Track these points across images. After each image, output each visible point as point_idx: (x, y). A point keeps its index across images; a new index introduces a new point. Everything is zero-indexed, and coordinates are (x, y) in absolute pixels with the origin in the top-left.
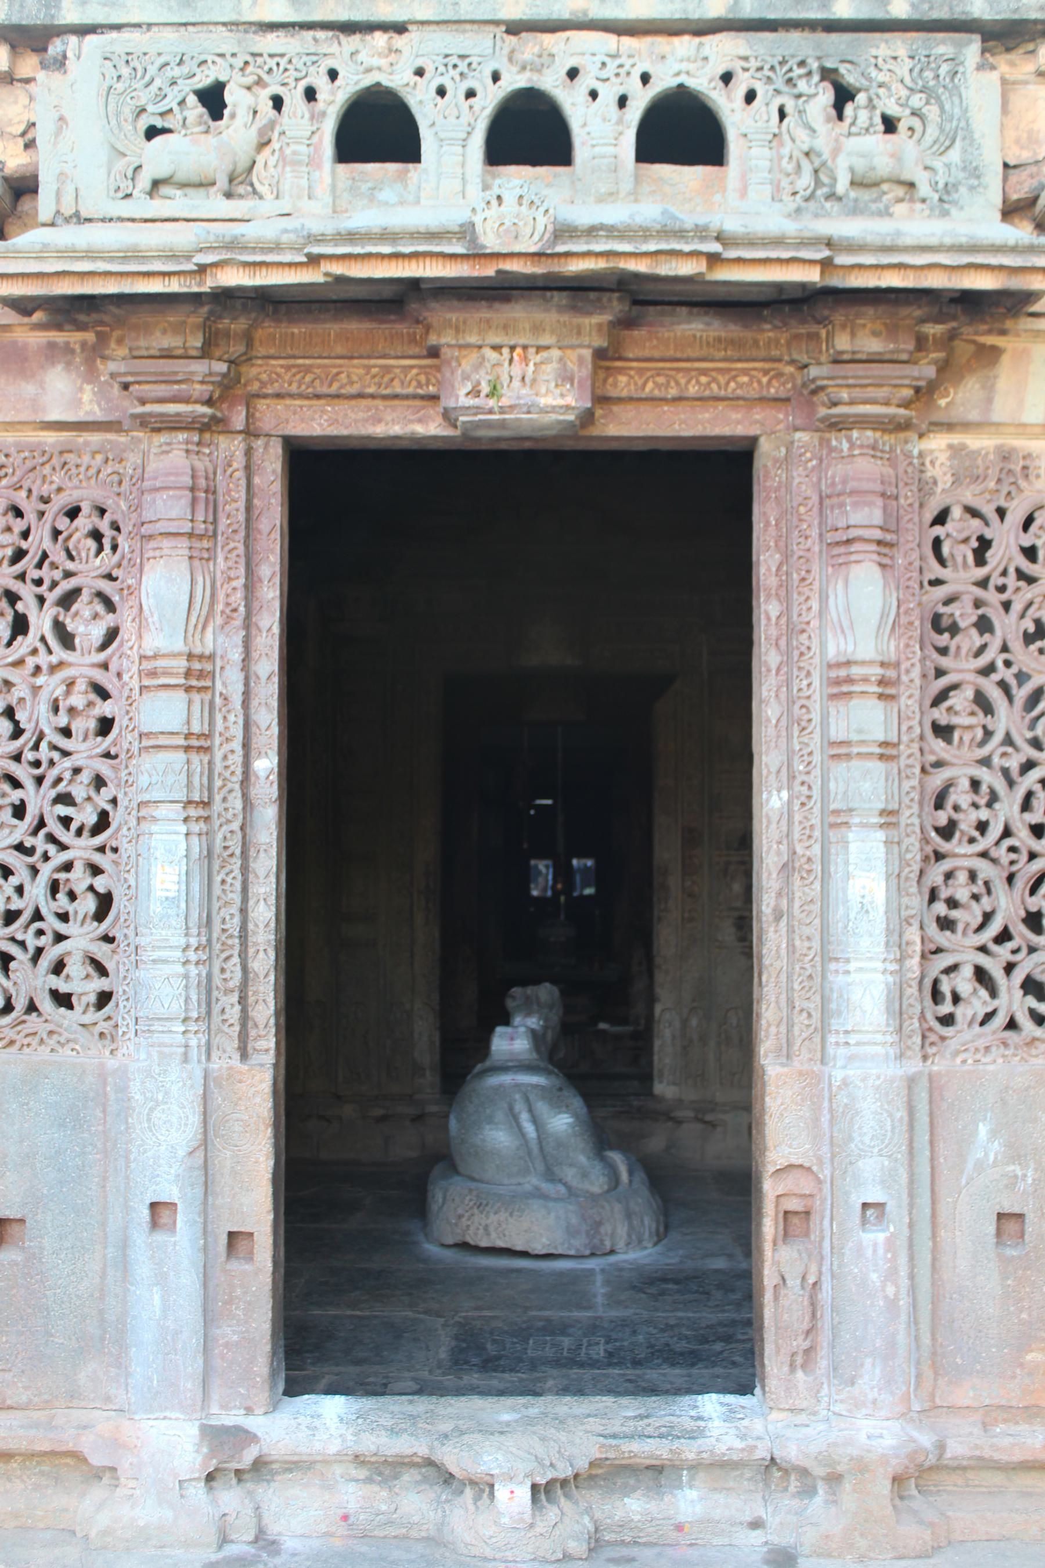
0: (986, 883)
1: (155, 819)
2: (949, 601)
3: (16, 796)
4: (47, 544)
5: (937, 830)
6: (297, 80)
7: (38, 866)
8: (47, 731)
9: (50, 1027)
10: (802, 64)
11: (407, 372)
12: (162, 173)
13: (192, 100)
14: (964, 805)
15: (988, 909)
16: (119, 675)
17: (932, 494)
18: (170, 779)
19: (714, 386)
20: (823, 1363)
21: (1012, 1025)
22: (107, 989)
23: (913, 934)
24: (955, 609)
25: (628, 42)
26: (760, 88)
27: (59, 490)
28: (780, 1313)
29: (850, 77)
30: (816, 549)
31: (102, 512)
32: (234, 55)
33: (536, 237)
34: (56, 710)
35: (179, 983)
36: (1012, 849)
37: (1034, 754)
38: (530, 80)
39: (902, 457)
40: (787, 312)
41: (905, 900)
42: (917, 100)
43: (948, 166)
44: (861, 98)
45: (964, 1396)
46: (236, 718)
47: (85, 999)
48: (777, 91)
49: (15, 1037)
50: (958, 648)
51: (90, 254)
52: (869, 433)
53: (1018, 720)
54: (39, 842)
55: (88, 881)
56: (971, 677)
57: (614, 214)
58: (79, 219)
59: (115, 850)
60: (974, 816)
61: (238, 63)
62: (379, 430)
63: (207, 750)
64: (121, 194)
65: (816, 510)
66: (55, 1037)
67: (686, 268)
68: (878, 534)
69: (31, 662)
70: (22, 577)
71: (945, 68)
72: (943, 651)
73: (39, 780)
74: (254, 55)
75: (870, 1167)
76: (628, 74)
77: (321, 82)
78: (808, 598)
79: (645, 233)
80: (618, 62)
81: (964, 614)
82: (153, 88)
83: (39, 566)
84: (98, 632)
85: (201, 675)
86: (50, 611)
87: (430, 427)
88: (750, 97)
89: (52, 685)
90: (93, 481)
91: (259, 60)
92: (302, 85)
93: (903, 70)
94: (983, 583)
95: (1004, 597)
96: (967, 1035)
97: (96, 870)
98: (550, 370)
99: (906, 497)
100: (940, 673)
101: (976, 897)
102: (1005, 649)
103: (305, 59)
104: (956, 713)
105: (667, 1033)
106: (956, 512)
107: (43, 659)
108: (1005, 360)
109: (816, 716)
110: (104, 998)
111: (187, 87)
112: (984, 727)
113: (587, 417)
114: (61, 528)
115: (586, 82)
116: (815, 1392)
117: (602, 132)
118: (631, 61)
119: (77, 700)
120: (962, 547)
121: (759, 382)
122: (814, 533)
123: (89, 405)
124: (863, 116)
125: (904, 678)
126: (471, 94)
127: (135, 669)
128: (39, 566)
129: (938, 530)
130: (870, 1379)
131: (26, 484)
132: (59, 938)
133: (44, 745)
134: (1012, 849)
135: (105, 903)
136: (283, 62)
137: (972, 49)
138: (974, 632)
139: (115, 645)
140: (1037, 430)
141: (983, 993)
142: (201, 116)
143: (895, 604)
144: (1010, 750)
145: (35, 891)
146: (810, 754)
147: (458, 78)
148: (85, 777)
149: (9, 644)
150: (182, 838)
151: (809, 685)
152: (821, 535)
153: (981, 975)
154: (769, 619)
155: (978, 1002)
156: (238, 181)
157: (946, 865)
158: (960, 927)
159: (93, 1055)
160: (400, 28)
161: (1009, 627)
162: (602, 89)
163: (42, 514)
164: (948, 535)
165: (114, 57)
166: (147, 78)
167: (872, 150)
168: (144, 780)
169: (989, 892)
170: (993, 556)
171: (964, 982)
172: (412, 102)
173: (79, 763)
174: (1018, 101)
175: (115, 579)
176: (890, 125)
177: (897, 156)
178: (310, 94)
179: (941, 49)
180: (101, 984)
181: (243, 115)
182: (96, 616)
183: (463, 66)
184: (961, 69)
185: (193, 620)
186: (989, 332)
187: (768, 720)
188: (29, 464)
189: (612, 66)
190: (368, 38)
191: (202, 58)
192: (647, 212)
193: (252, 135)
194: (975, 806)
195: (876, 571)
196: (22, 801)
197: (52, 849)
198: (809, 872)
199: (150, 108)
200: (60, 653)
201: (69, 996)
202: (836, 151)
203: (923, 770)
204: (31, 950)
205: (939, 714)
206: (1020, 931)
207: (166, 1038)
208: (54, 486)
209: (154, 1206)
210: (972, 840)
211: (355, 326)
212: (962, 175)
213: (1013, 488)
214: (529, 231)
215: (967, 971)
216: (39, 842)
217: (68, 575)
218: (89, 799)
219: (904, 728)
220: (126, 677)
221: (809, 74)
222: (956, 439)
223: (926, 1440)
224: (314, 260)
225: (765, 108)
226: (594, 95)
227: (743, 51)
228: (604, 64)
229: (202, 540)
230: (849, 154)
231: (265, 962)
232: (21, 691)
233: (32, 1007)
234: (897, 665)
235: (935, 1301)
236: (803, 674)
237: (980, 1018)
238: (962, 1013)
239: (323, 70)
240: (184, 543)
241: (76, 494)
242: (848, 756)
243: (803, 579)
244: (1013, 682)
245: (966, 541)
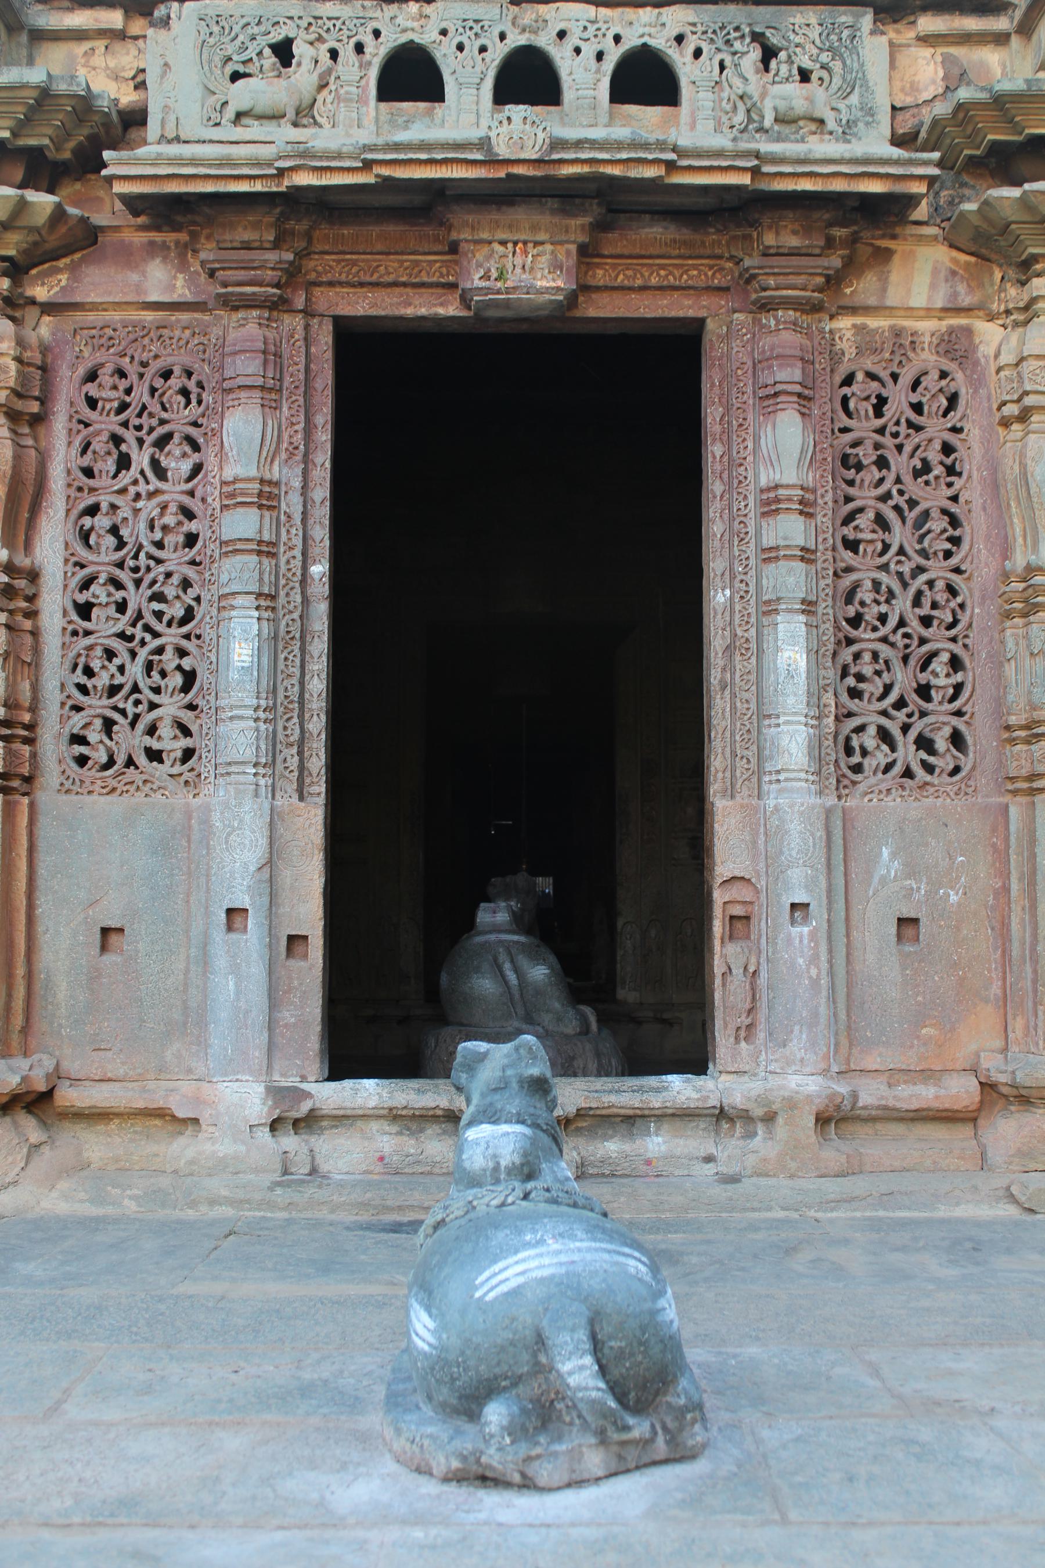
0: (886, 662)
1: (233, 607)
2: (855, 444)
3: (119, 595)
4: (146, 398)
5: (848, 621)
6: (349, 37)
7: (137, 650)
8: (145, 543)
9: (144, 777)
10: (737, 29)
11: (432, 266)
12: (244, 106)
13: (267, 52)
14: (868, 602)
15: (888, 682)
16: (203, 500)
17: (840, 362)
18: (246, 575)
19: (671, 278)
20: (761, 1035)
21: (908, 773)
22: (191, 746)
23: (829, 699)
24: (860, 451)
26: (705, 47)
27: (156, 357)
28: (727, 996)
29: (774, 40)
30: (751, 402)
31: (189, 374)
32: (300, 18)
33: (537, 148)
34: (152, 528)
35: (251, 734)
36: (906, 636)
37: (922, 561)
38: (529, 39)
39: (816, 333)
40: (729, 213)
41: (823, 672)
42: (825, 57)
43: (849, 107)
44: (783, 55)
45: (872, 1062)
46: (297, 531)
47: (173, 755)
48: (718, 50)
49: (116, 785)
50: (862, 480)
51: (193, 162)
52: (791, 313)
53: (909, 535)
54: (138, 632)
55: (177, 661)
56: (872, 503)
57: (597, 133)
58: (177, 139)
59: (198, 637)
60: (875, 609)
61: (304, 24)
62: (409, 312)
63: (273, 555)
64: (211, 123)
65: (750, 372)
66: (149, 785)
67: (650, 172)
68: (798, 388)
69: (132, 490)
70: (125, 424)
71: (846, 33)
72: (851, 483)
73: (138, 583)
74: (315, 18)
75: (796, 875)
76: (604, 35)
77: (368, 39)
78: (744, 440)
79: (619, 146)
80: (596, 26)
81: (866, 454)
82: (238, 42)
83: (140, 415)
84: (186, 466)
85: (270, 496)
86: (148, 451)
87: (450, 309)
88: (698, 53)
89: (149, 508)
90: (183, 351)
91: (320, 22)
92: (353, 41)
93: (814, 33)
94: (881, 431)
95: (897, 441)
96: (873, 780)
97: (182, 653)
98: (544, 261)
99: (820, 363)
100: (848, 499)
101: (878, 673)
102: (898, 481)
103: (355, 21)
104: (861, 531)
105: (629, 944)
106: (860, 376)
107: (142, 488)
108: (896, 259)
109: (751, 529)
110: (188, 754)
111: (263, 41)
112: (883, 541)
113: (572, 299)
114: (157, 385)
115: (572, 41)
116: (755, 1057)
117: (584, 79)
118: (606, 26)
119: (170, 520)
120: (864, 403)
121: (706, 275)
122: (749, 390)
123: (181, 290)
124: (784, 69)
125: (820, 501)
126: (483, 49)
127: (217, 493)
128: (140, 415)
129: (846, 390)
130: (798, 1044)
131: (129, 352)
132: (153, 706)
133: (142, 555)
134: (906, 636)
135: (190, 678)
136: (338, 24)
138: (874, 468)
139: (200, 476)
140: (922, 313)
141: (885, 748)
142: (274, 64)
143: (812, 443)
144: (903, 558)
145: (134, 669)
146: (747, 558)
147: (473, 37)
148: (175, 580)
149: (115, 476)
150: (255, 621)
151: (746, 506)
152: (754, 392)
153: (884, 735)
154: (714, 457)
155: (882, 756)
156: (304, 114)
157: (855, 648)
158: (866, 696)
159: (182, 798)
161: (901, 464)
162: (584, 47)
163: (141, 376)
164: (853, 394)
165: (208, 19)
166: (233, 34)
167: (791, 94)
168: (224, 578)
169: (889, 670)
170: (889, 410)
171: (870, 739)
172: (438, 55)
173: (171, 568)
174: (902, 59)
175: (201, 426)
176: (805, 76)
177: (810, 99)
178: (359, 48)
179: (843, 19)
180: (185, 742)
181: (307, 64)
182: (184, 455)
183: (477, 28)
184: (858, 34)
185: (264, 454)
186: (883, 237)
187: (715, 535)
188: (132, 337)
189: (592, 29)
190: (404, 6)
191: (276, 19)
192: (621, 132)
193: (315, 77)
194: (877, 602)
195: (798, 418)
196: (124, 599)
197: (148, 637)
198: (748, 649)
199: (235, 58)
200: (155, 483)
201: (160, 752)
202: (763, 95)
203: (835, 574)
204: (130, 716)
205: (848, 531)
206: (913, 698)
207: (241, 778)
208: (152, 354)
209: (230, 911)
210: (875, 629)
211: (392, 228)
212: (860, 114)
213: (903, 358)
214: (531, 143)
215: (872, 730)
216: (138, 632)
217: (163, 422)
218: (178, 597)
219: (820, 540)
220: (210, 500)
221: (743, 37)
222: (859, 320)
223: (842, 1088)
224: (368, 165)
225: (709, 63)
226: (578, 51)
227: (692, 19)
228: (585, 28)
229: (270, 393)
230: (774, 97)
231: (318, 724)
232: (125, 512)
233: (130, 762)
234: (814, 491)
235: (849, 985)
236: (741, 498)
237: (882, 767)
238: (869, 763)
239: (369, 30)
240: (257, 394)
241: (170, 360)
242: (777, 558)
243: (741, 425)
244: (905, 507)
245: (867, 398)
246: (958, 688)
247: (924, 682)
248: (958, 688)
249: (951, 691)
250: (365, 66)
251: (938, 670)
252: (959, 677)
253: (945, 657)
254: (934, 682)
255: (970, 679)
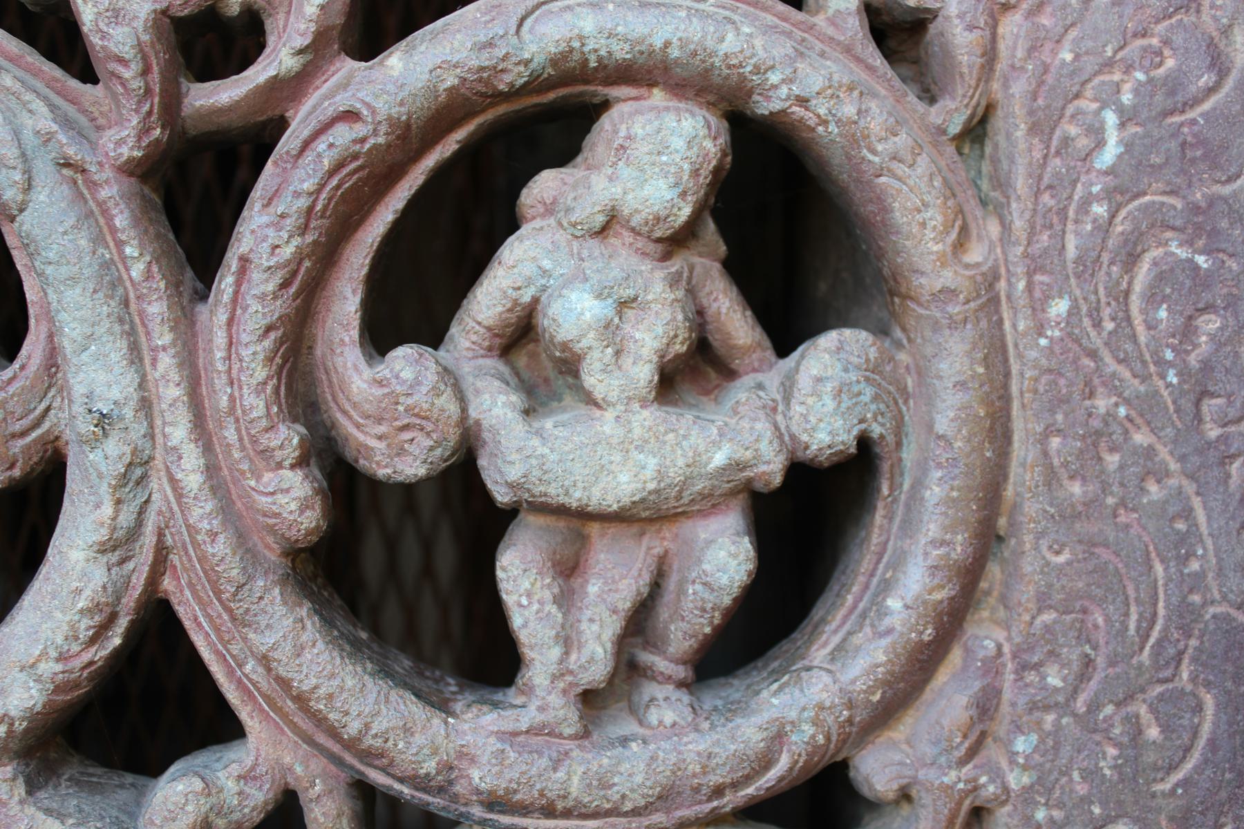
246: (809, 520)
247: (401, 458)
248: (809, 520)
249: (724, 558)
251: (574, 314)
252: (817, 395)
253: (655, 157)
254: (524, 453)
255: (949, 410)
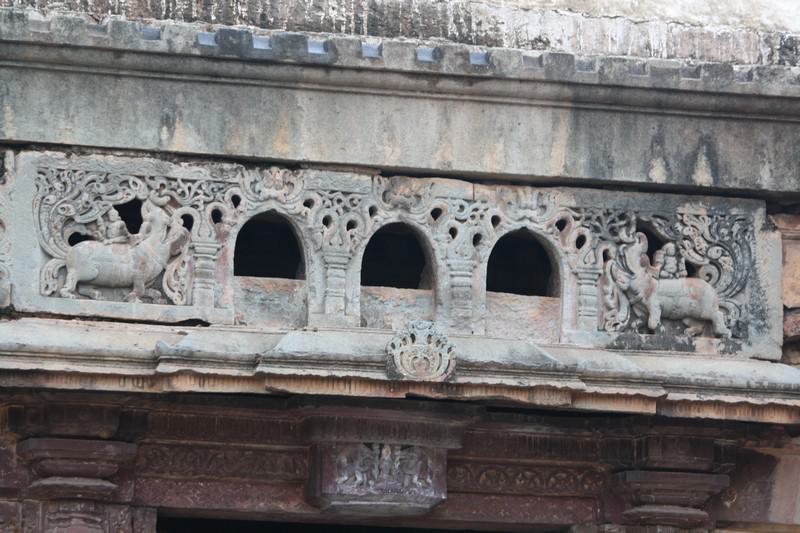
6: (206, 203)
10: (622, 217)
13: (114, 213)
19: (537, 480)
25: (483, 190)
32: (152, 178)
33: (442, 370)
38: (400, 217)
42: (714, 252)
43: (739, 308)
48: (602, 239)
61: (156, 184)
62: (245, 506)
64: (49, 292)
71: (736, 228)
74: (169, 179)
76: (482, 216)
77: (226, 207)
80: (474, 206)
82: (80, 202)
88: (580, 241)
91: (174, 184)
92: (211, 207)
93: (704, 227)
103: (213, 185)
108: (780, 469)
111: (109, 201)
115: (448, 221)
117: (460, 261)
118: (484, 206)
121: (575, 478)
124: (672, 262)
126: (351, 225)
136: (194, 188)
137: (759, 217)
142: (121, 228)
147: (341, 211)
160: (294, 166)
162: (461, 228)
165: (49, 175)
166: (76, 192)
178: (217, 216)
179: (734, 211)
183: (346, 200)
184: (751, 229)
186: (768, 445)
189: (469, 209)
190: (266, 171)
191: (124, 178)
199: (78, 219)
202: (649, 292)
212: (751, 316)
214: (436, 365)
221: (628, 225)
226: (453, 232)
227: (573, 204)
228: (462, 207)
230: (660, 294)
239: (228, 196)
250: (222, 236)
